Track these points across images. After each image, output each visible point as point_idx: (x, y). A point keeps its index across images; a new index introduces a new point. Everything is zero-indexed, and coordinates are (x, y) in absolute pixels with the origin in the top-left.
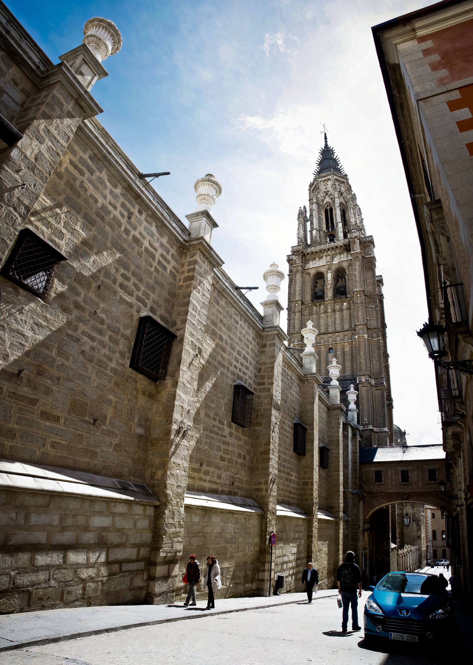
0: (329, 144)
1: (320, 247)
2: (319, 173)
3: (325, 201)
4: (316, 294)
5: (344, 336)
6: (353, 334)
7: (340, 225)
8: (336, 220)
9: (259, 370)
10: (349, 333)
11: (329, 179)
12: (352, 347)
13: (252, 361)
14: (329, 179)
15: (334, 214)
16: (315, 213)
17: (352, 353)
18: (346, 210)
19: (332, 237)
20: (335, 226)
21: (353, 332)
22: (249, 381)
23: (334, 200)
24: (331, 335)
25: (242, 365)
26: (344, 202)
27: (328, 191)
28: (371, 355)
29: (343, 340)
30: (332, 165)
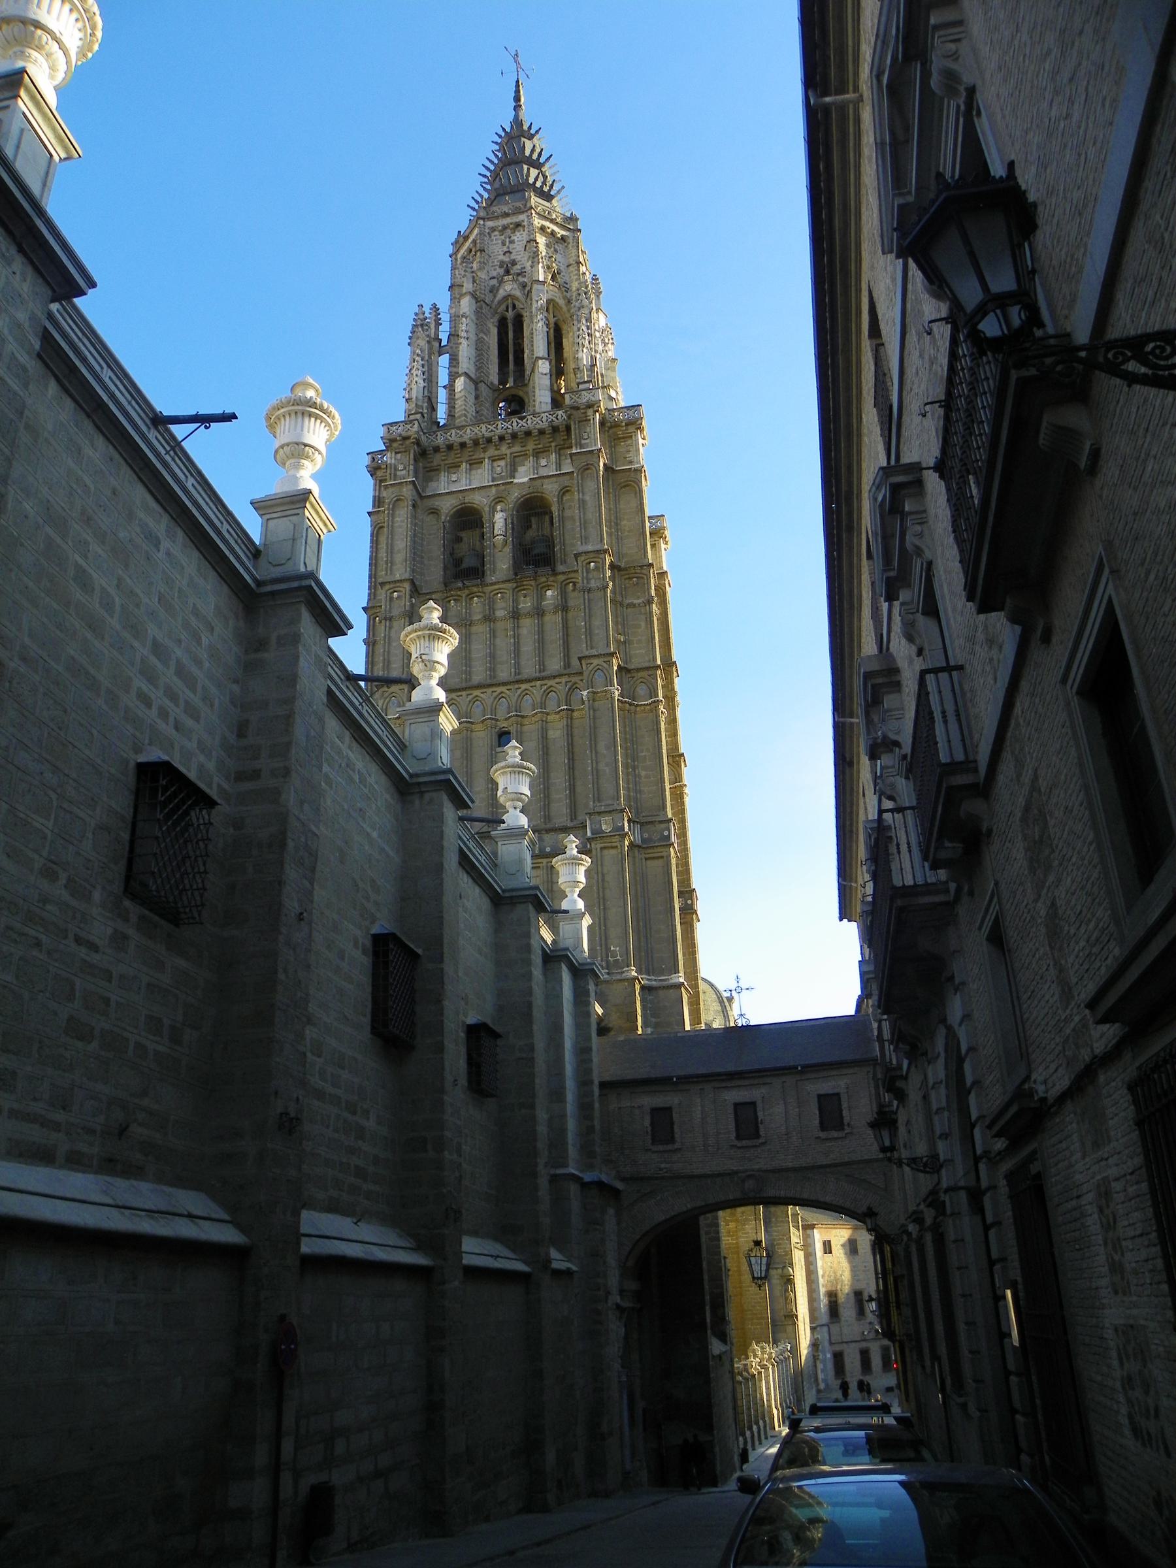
1: (476, 430)
2: (491, 202)
3: (501, 293)
4: (458, 562)
5: (547, 693)
6: (573, 688)
7: (544, 367)
9: (241, 730)
10: (561, 686)
11: (518, 225)
12: (570, 729)
13: (213, 690)
14: (518, 225)
15: (526, 333)
16: (466, 327)
17: (571, 745)
18: (565, 328)
19: (518, 405)
20: (528, 372)
21: (574, 679)
22: (199, 757)
23: (530, 291)
24: (503, 689)
25: (174, 698)
26: (561, 302)
27: (514, 263)
29: (543, 705)
30: (531, 181)
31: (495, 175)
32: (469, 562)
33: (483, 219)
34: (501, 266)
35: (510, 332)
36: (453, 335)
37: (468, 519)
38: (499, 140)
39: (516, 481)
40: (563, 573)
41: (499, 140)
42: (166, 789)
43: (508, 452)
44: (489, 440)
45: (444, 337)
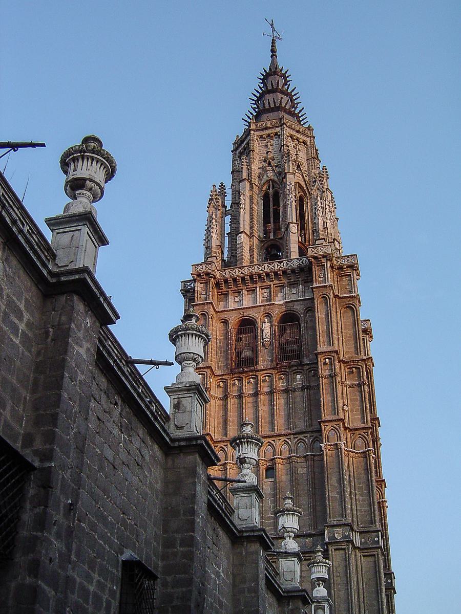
0: (281, 63)
5: (297, 443)
7: (294, 228)
8: (285, 216)
21: (315, 435)
28: (353, 484)
31: (259, 99)
32: (247, 353)
33: (254, 130)
34: (265, 161)
35: (272, 202)
36: (236, 203)
37: (247, 325)
38: (262, 77)
39: (276, 303)
40: (307, 364)
41: (262, 77)
42: (138, 575)
43: (272, 283)
44: (260, 276)
45: (228, 204)
